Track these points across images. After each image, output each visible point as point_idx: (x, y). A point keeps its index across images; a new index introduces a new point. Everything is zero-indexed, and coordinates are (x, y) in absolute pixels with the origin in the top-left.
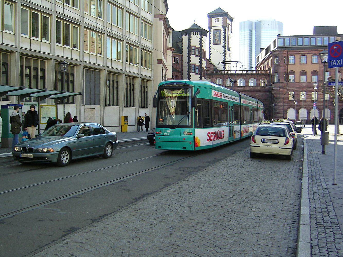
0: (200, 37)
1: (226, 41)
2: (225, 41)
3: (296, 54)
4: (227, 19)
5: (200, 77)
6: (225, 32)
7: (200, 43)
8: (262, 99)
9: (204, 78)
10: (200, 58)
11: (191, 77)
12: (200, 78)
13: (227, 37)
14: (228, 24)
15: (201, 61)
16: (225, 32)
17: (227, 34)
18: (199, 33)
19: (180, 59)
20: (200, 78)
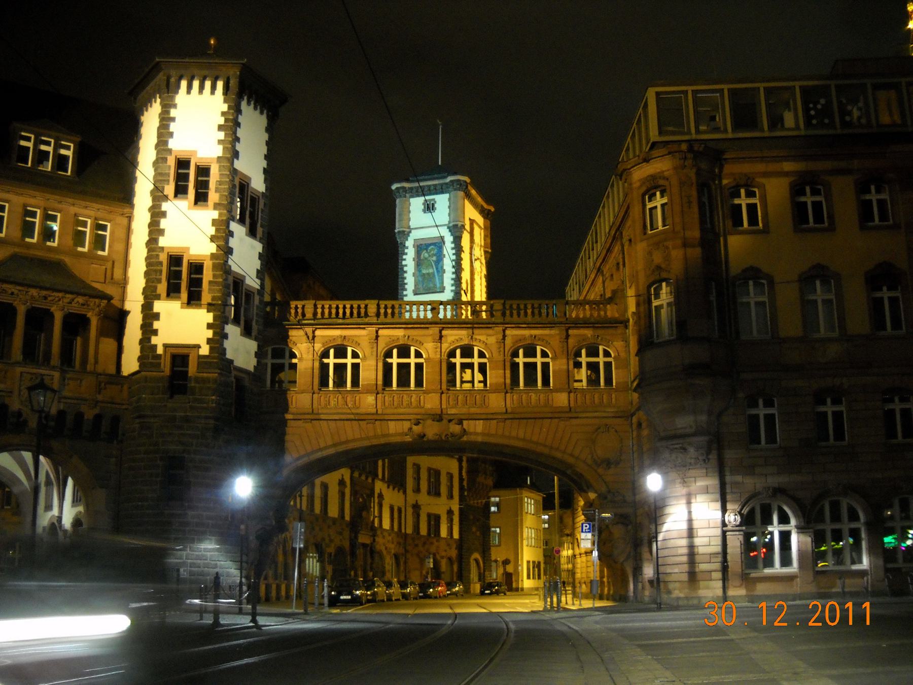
0: (225, 107)
1: (464, 281)
2: (458, 280)
3: (766, 175)
4: (467, 203)
5: (211, 320)
6: (458, 249)
7: (221, 135)
8: (589, 461)
9: (247, 332)
10: (215, 214)
11: (156, 325)
12: (209, 326)
13: (466, 264)
14: (472, 222)
15: (223, 236)
16: (458, 249)
17: (465, 256)
18: (220, 85)
19: (121, 233)
20: (209, 326)
